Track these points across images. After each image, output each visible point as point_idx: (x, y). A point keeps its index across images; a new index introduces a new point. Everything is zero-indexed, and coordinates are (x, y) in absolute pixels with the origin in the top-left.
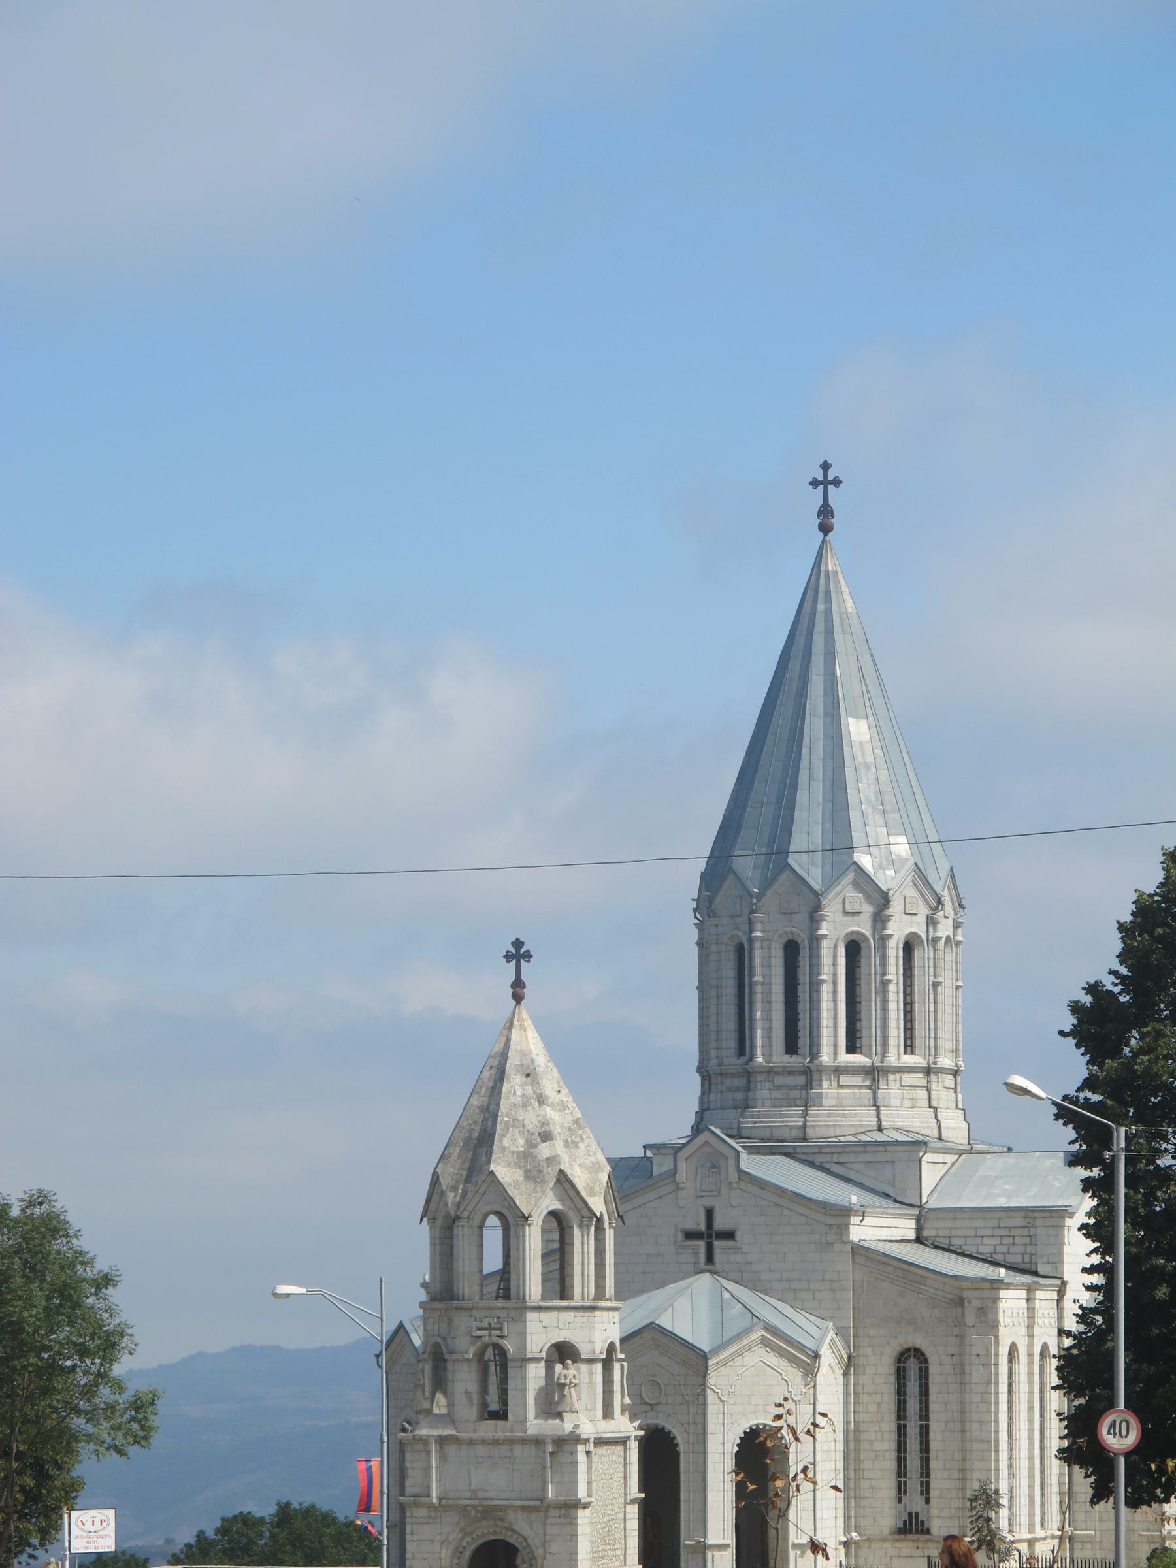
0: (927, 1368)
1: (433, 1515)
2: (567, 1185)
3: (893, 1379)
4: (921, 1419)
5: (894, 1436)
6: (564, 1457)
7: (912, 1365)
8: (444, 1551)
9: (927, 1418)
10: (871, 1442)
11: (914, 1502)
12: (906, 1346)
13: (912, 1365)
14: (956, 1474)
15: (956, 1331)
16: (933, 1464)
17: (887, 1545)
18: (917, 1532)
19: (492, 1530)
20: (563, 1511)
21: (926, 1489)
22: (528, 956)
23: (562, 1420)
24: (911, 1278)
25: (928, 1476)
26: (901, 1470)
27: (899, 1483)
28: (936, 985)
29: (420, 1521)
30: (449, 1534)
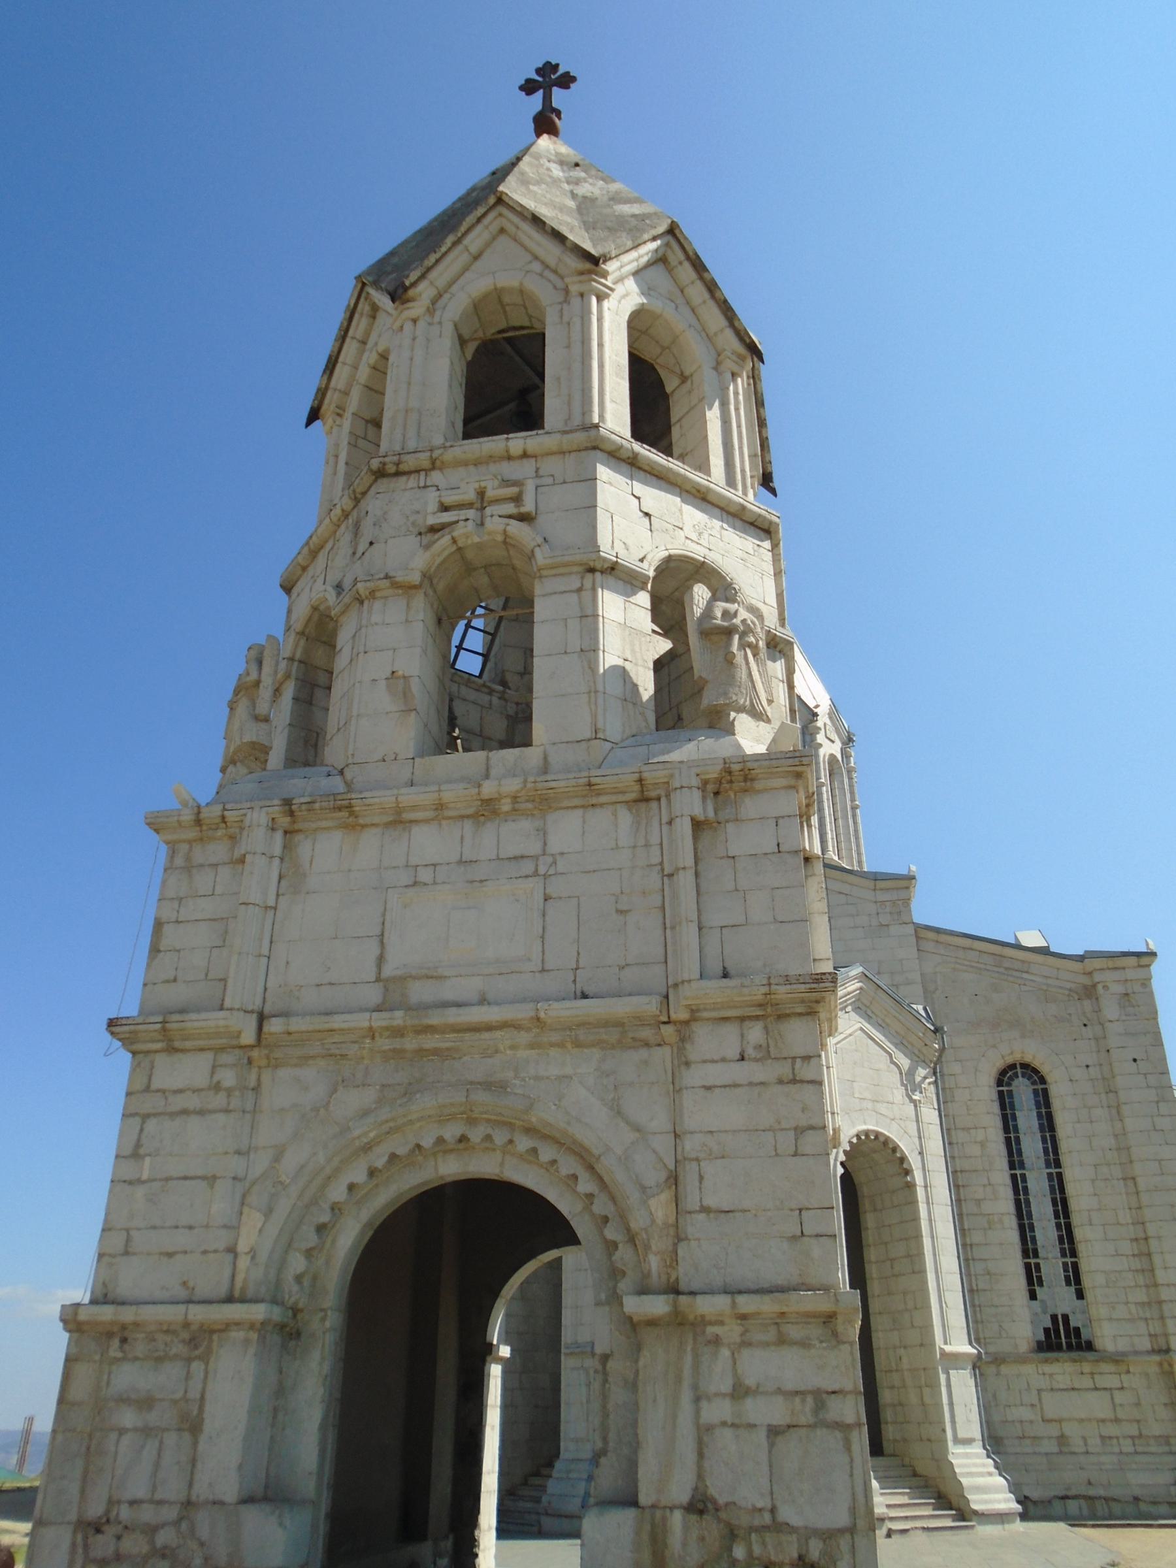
0: (1045, 1092)
1: (228, 1078)
2: (686, 272)
3: (996, 1108)
4: (1048, 1165)
5: (1009, 1193)
6: (746, 838)
7: (1022, 1089)
8: (253, 1220)
9: (1058, 1164)
10: (978, 1202)
11: (1059, 1297)
12: (1010, 1060)
13: (1022, 1089)
14: (1126, 1247)
15: (1088, 1032)
16: (1078, 1233)
17: (1029, 1369)
18: (1070, 1347)
19: (451, 1132)
20: (755, 1033)
21: (1074, 1277)
22: (566, 81)
23: (730, 730)
24: (1007, 965)
25: (1074, 1253)
26: (1029, 1249)
27: (1028, 1267)
28: (854, 808)
29: (178, 1102)
30: (279, 1154)
